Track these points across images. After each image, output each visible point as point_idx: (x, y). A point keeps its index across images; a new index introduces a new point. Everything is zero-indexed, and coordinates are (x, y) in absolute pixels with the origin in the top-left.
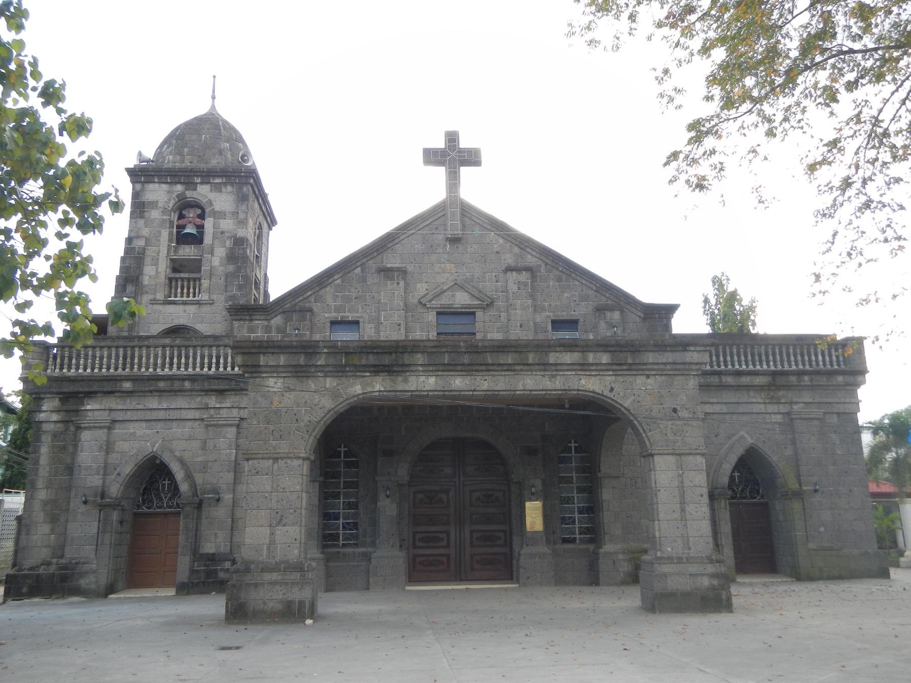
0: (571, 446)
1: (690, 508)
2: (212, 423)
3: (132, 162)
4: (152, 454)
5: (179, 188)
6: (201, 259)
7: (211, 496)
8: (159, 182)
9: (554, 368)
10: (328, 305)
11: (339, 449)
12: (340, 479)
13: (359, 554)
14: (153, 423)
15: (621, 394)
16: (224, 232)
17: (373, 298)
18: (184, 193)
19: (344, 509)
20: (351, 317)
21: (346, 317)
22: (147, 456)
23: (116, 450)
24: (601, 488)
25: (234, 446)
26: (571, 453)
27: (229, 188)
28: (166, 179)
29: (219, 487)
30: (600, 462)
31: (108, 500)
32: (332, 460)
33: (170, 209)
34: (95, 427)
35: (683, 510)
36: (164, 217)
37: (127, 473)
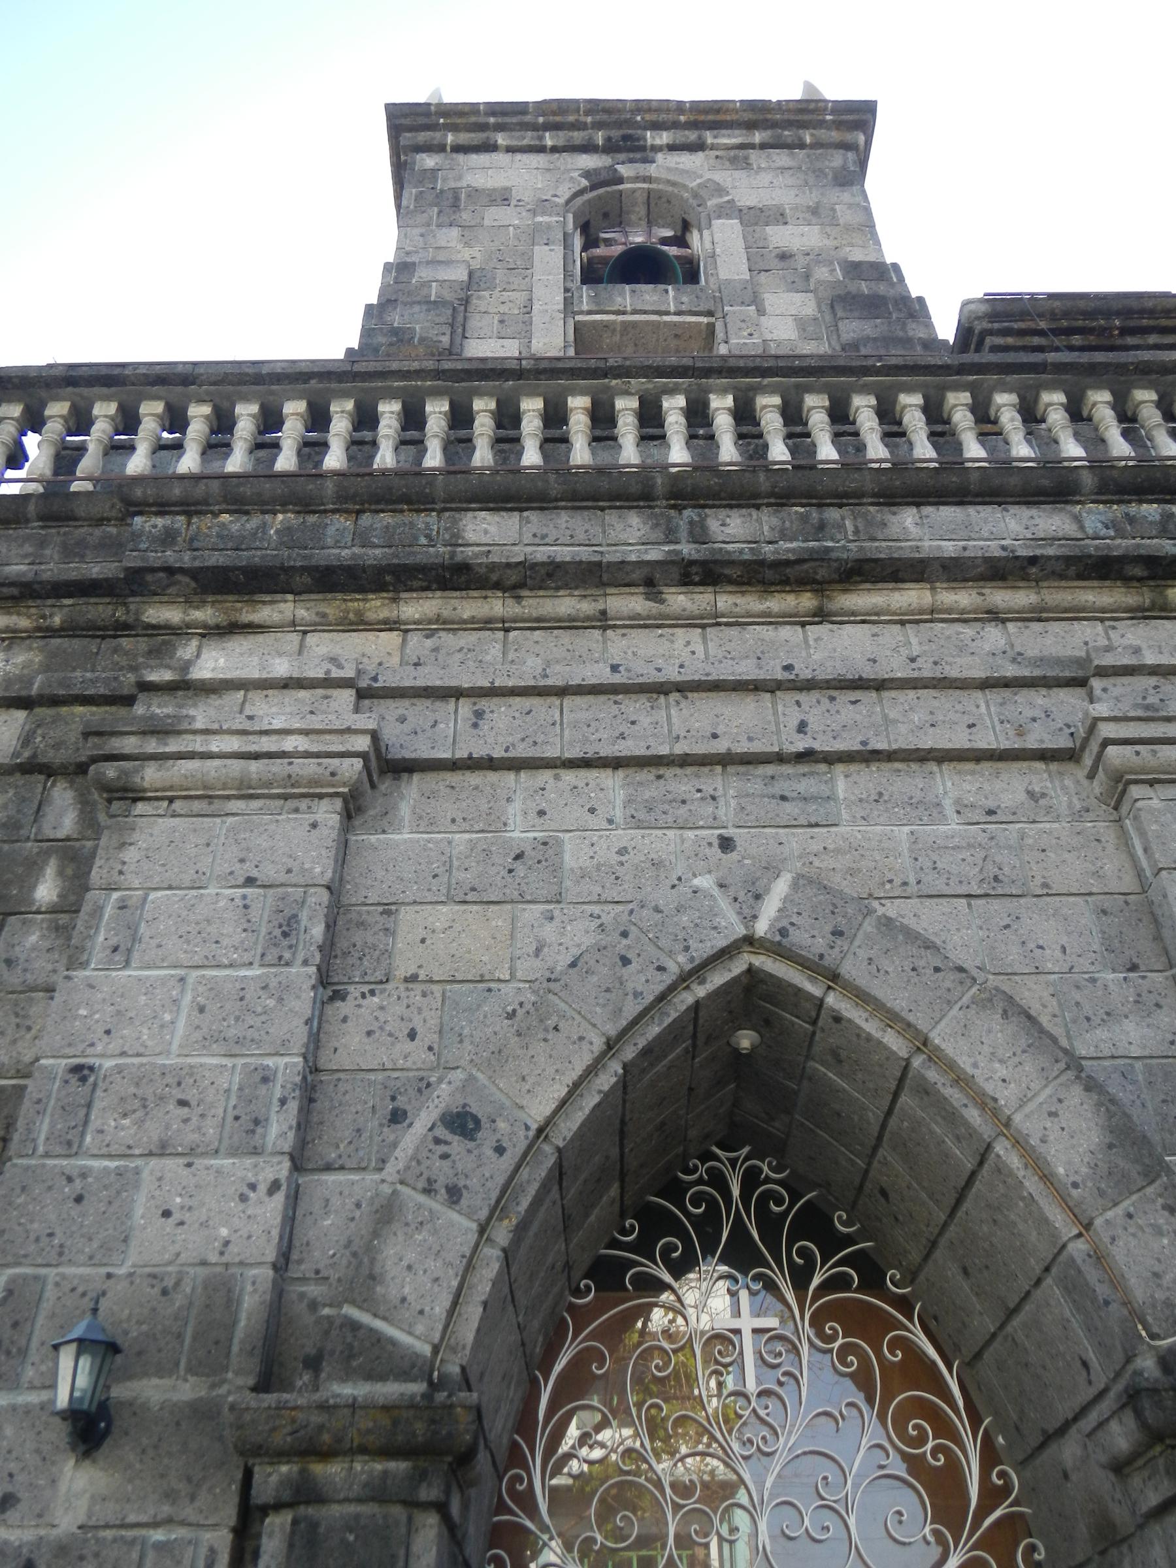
4: (737, 967)
6: (711, 328)
8: (510, 150)
14: (681, 783)
16: (791, 256)
22: (698, 972)
23: (403, 969)
27: (781, 158)
28: (541, 138)
31: (347, 1390)
34: (246, 791)
36: (539, 219)
37: (539, 1109)
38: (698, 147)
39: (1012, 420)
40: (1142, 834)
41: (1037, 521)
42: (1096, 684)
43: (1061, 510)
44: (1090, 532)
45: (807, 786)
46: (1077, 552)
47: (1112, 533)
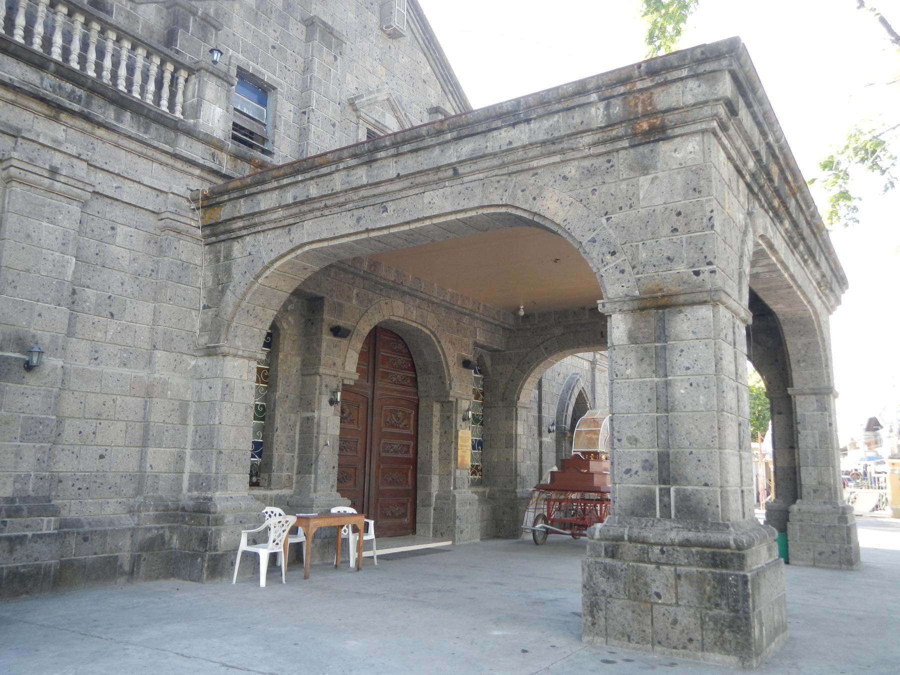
2: (31, 177)
7: (11, 354)
10: (234, 35)
13: (271, 498)
17: (296, 62)
20: (267, 76)
21: (260, 72)
24: (517, 419)
25: (71, 248)
30: (522, 387)
39: (43, 11)
40: (10, 198)
41: (28, 73)
42: (20, 140)
43: (38, 72)
44: (44, 86)
46: (35, 92)
47: (51, 90)
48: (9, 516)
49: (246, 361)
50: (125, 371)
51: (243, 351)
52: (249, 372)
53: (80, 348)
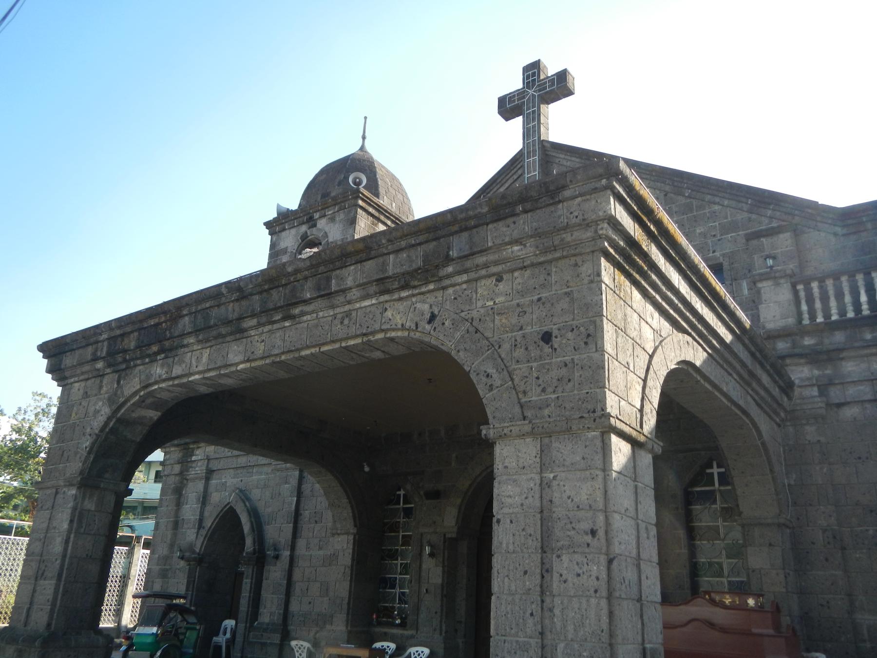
0: (712, 474)
1: (564, 565)
3: (272, 215)
5: (304, 228)
9: (341, 299)
11: (398, 493)
12: (399, 532)
15: (447, 323)
18: (306, 232)
19: (400, 574)
26: (713, 485)
29: (280, 542)
32: (392, 507)
33: (294, 251)
35: (546, 571)
38: (325, 216)
45: (251, 470)
48: (263, 632)
49: (346, 536)
50: (321, 552)
51: (341, 530)
52: (348, 543)
53: (301, 543)
